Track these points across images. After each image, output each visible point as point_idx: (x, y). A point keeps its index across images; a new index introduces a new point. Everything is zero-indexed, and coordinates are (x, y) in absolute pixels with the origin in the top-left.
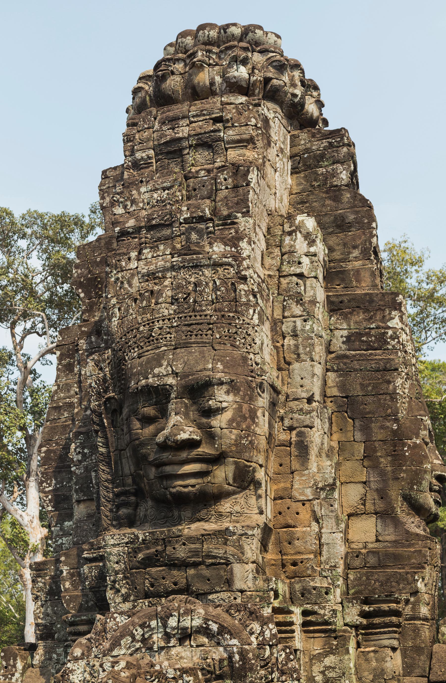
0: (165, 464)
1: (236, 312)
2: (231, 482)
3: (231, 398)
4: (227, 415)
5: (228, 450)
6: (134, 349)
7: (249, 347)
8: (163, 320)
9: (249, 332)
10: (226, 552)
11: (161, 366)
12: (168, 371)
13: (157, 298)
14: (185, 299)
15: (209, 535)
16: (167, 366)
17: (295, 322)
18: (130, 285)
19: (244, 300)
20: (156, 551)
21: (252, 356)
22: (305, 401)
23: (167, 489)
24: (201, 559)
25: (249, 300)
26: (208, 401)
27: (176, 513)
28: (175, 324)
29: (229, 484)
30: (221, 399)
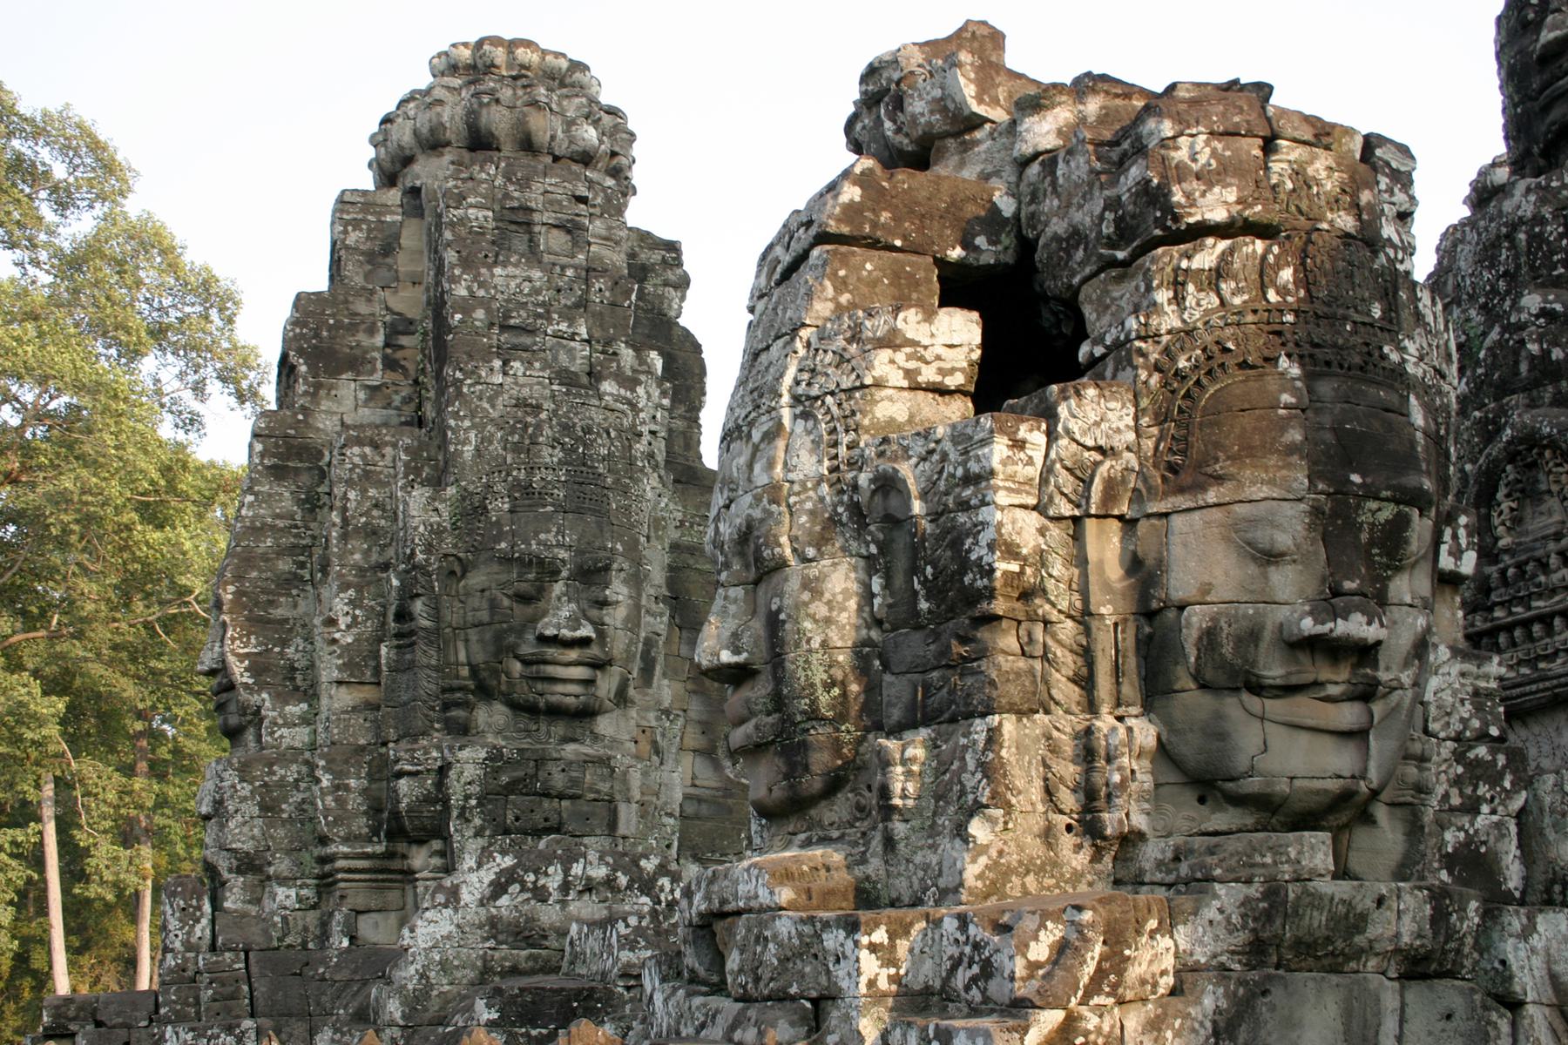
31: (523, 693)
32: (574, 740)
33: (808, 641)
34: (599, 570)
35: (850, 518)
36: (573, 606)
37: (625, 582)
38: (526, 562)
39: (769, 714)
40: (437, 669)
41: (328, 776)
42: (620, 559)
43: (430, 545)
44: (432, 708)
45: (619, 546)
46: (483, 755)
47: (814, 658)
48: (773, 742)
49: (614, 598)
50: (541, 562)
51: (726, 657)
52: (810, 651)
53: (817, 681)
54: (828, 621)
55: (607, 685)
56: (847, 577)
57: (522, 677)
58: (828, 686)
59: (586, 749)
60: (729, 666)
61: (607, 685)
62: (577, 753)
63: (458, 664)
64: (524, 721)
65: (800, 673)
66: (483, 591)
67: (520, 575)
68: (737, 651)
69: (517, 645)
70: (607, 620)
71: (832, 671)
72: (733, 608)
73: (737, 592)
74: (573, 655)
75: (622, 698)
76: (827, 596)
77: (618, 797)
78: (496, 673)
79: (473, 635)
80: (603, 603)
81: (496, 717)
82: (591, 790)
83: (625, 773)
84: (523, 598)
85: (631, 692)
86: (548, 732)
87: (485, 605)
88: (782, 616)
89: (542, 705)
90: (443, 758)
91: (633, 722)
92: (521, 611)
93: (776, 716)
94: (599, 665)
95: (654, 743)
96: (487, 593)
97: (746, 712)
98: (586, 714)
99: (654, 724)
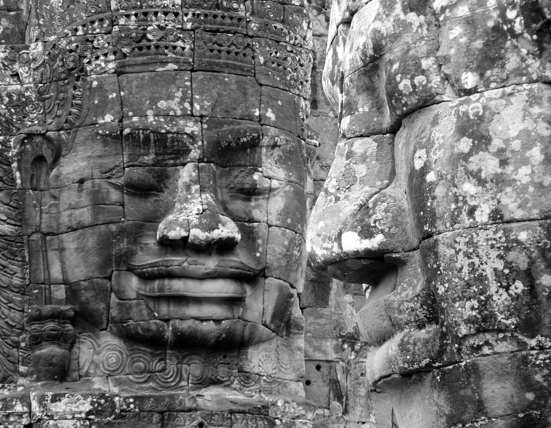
0: (171, 276)
1: (283, 22)
2: (268, 319)
5: (275, 264)
6: (106, 55)
9: (302, 62)
15: (243, 412)
16: (183, 100)
26: (251, 173)
28: (189, 26)
29: (265, 325)
30: (271, 174)
31: (141, 319)
32: (215, 382)
33: (471, 212)
34: (243, 147)
35: (527, 26)
36: (207, 197)
37: (282, 161)
38: (138, 141)
39: (420, 326)
40: (22, 290)
42: (273, 131)
44: (16, 345)
45: (270, 114)
46: (87, 407)
47: (481, 237)
48: (428, 368)
49: (266, 183)
50: (161, 139)
51: (353, 243)
52: (474, 227)
53: (489, 272)
54: (500, 181)
55: (260, 305)
56: (526, 114)
57: (140, 297)
58: (504, 281)
59: (233, 395)
60: (358, 256)
61: (260, 305)
62: (220, 401)
63: (49, 282)
64: (144, 359)
65: (462, 261)
66: (81, 181)
67: (133, 157)
68: (367, 232)
69: (130, 254)
70: (257, 214)
71: (512, 256)
72: (361, 170)
73: (365, 146)
74: (211, 263)
75: (283, 323)
76: (497, 143)
78: (103, 294)
79: (70, 241)
80: (250, 193)
81: (104, 354)
84: (140, 190)
85: (296, 312)
86: (179, 373)
87: (85, 199)
88: (431, 177)
89: (168, 334)
90: (30, 413)
91: (300, 356)
92: (135, 208)
93: (433, 328)
94: (250, 278)
95: (334, 384)
96: (88, 184)
97: (386, 323)
98: (230, 347)
99: (333, 356)
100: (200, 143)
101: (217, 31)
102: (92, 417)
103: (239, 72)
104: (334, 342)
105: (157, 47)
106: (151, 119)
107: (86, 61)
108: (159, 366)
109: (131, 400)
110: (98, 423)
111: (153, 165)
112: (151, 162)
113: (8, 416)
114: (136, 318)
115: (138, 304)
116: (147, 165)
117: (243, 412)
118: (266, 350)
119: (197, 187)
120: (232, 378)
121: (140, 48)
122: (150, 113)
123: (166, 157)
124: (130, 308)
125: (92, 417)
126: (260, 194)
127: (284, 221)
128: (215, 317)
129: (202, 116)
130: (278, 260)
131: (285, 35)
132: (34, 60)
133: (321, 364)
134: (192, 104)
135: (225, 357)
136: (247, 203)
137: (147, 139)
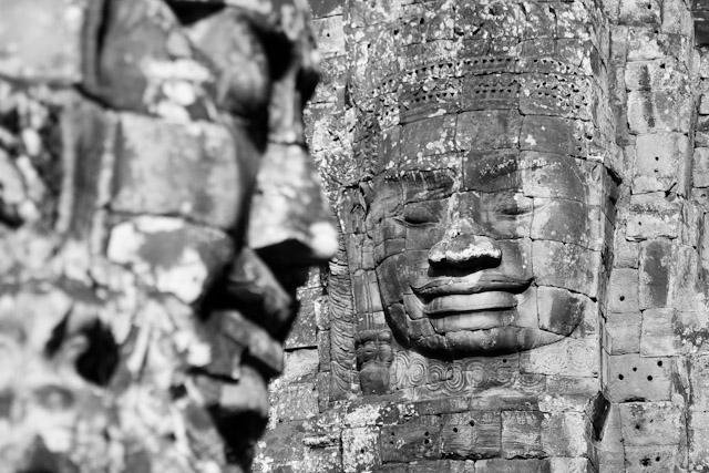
3: (546, 191)
4: (541, 219)
5: (543, 274)
7: (576, 111)
8: (441, 66)
9: (576, 88)
10: (539, 438)
11: (437, 138)
12: (449, 147)
13: (431, 31)
14: (474, 33)
16: (447, 139)
17: (646, 68)
18: (387, 9)
19: (569, 35)
20: (427, 434)
21: (579, 124)
22: (663, 194)
23: (443, 334)
24: (498, 449)
25: (577, 37)
27: (458, 375)
28: (459, 74)
30: (533, 193)
32: (496, 384)
34: (503, 173)
41: (269, 460)
43: (334, 179)
49: (527, 203)
61: (534, 310)
70: (520, 231)
74: (472, 279)
77: (549, 450)
80: (514, 212)
82: (511, 444)
83: (559, 420)
84: (415, 222)
86: (464, 378)
98: (507, 350)
99: (672, 351)
100: (460, 175)
101: (485, 74)
102: (381, 423)
103: (503, 107)
104: (673, 338)
105: (430, 97)
106: (420, 159)
107: (379, 118)
108: (449, 375)
109: (412, 406)
110: (387, 428)
111: (428, 200)
112: (425, 197)
113: (331, 428)
114: (425, 334)
115: (425, 322)
116: (421, 200)
117: (512, 410)
118: (552, 352)
119: (458, 213)
120: (512, 379)
121: (418, 100)
122: (420, 154)
123: (438, 191)
124: (419, 326)
125: (381, 423)
126: (522, 212)
127: (547, 234)
128: (484, 326)
129: (463, 151)
130: (546, 270)
131: (555, 67)
132: (349, 123)
133: (662, 359)
134: (454, 142)
135: (505, 361)
136: (513, 222)
137: (418, 176)
